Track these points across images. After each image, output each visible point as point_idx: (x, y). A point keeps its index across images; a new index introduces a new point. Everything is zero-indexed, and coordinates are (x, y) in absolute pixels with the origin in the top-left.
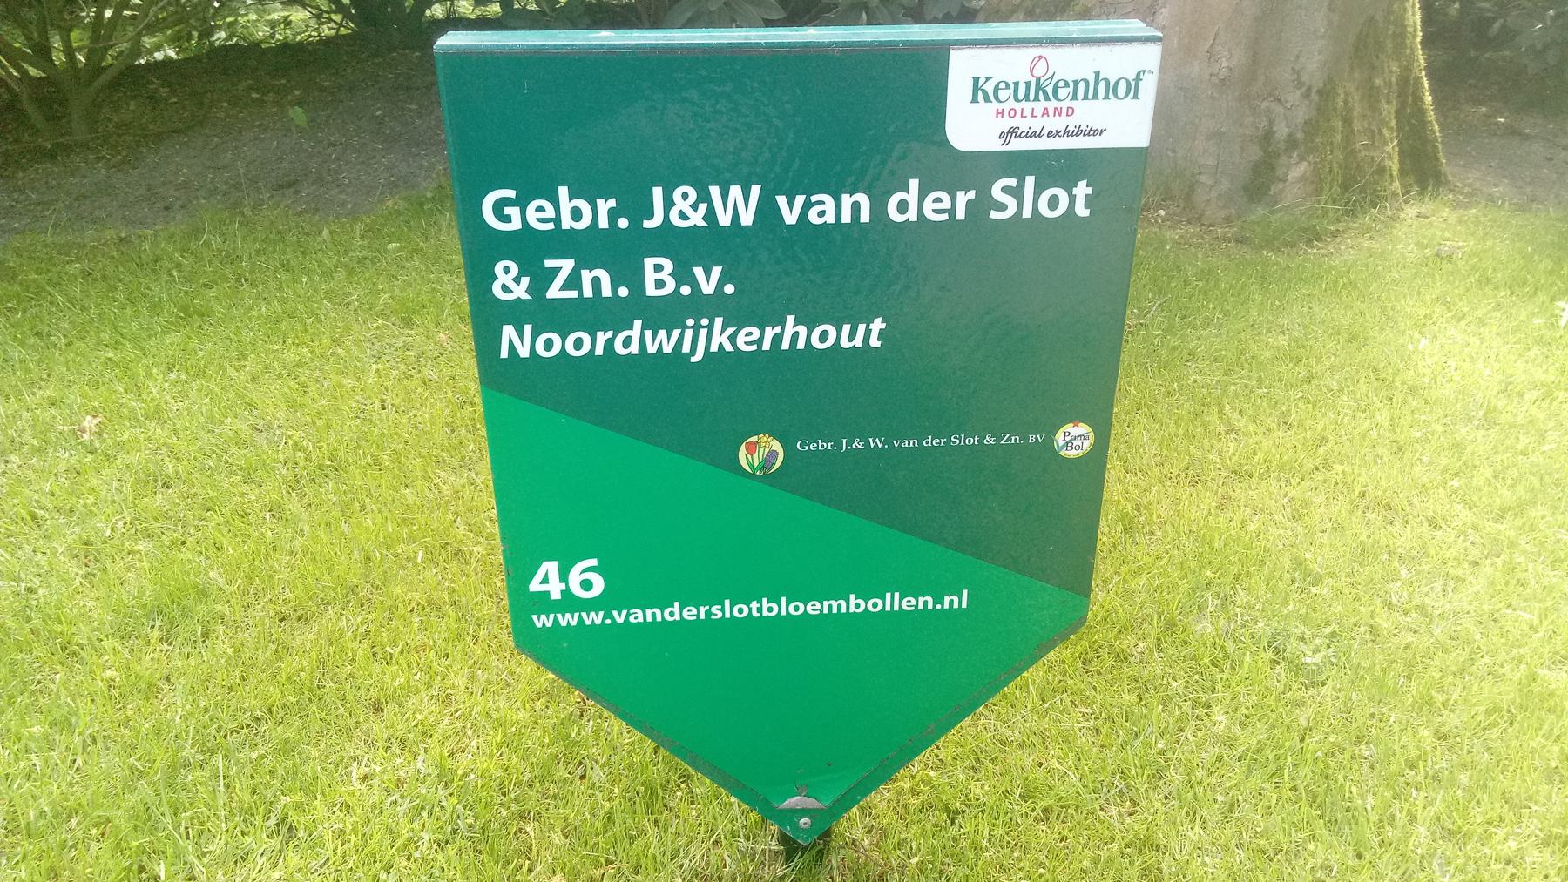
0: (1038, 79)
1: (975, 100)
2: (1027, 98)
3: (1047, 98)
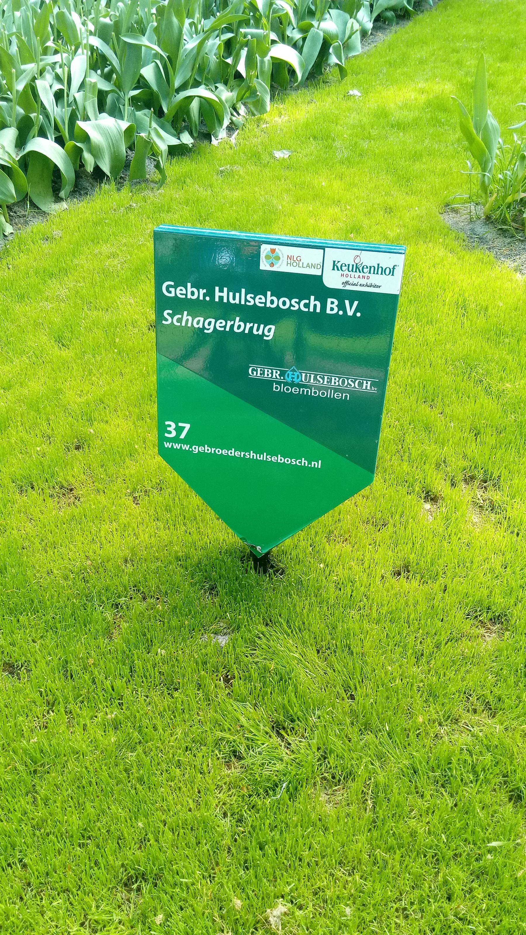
1: (333, 269)
2: (352, 271)
3: (360, 272)
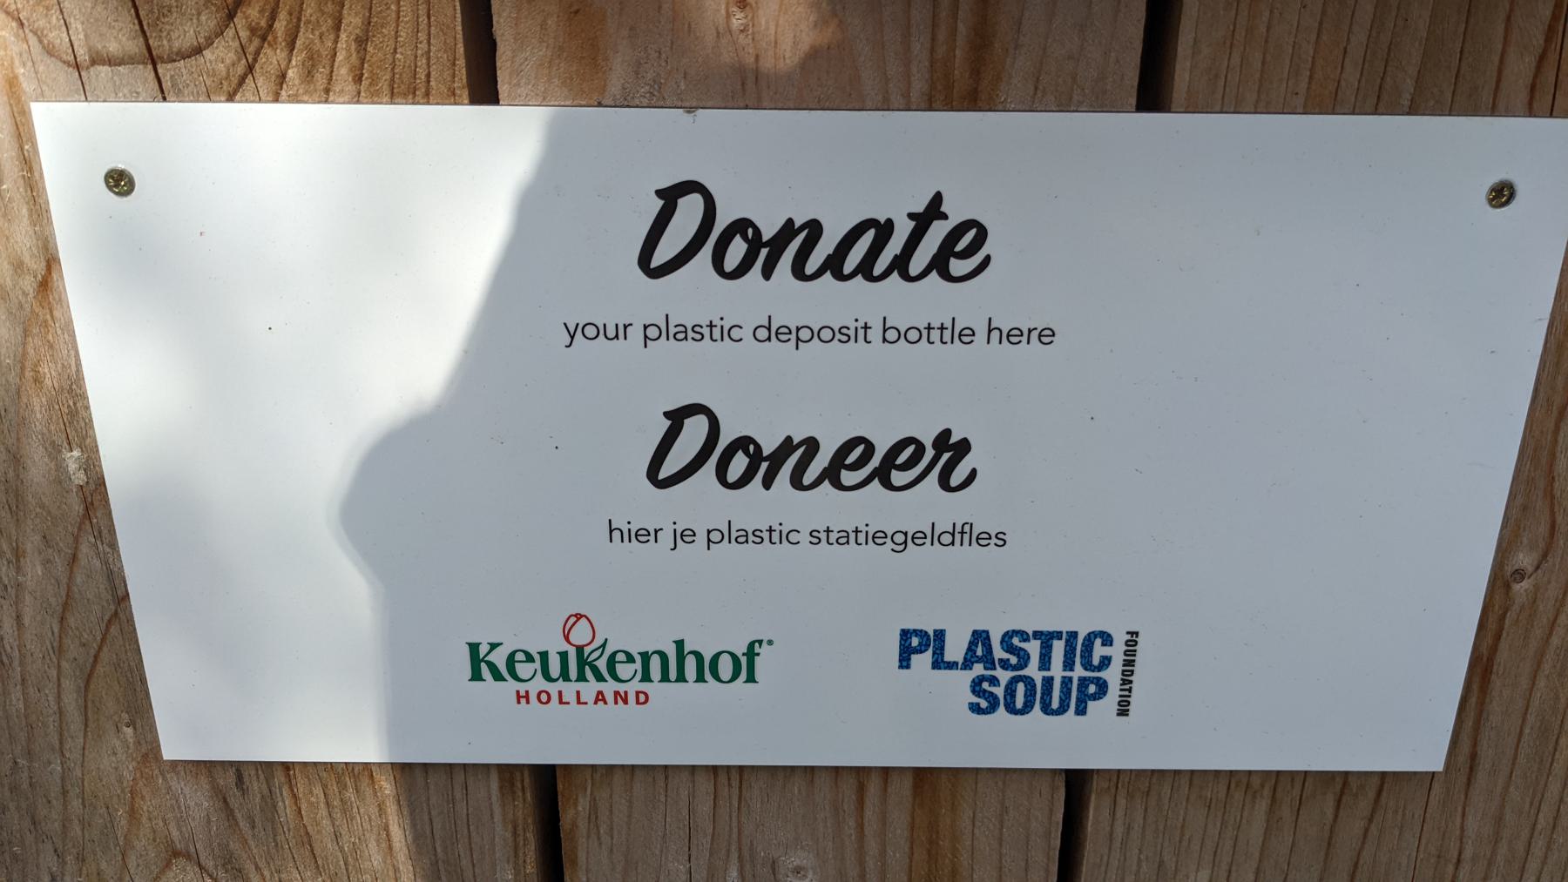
0: (580, 649)
1: (476, 676)
3: (600, 678)
